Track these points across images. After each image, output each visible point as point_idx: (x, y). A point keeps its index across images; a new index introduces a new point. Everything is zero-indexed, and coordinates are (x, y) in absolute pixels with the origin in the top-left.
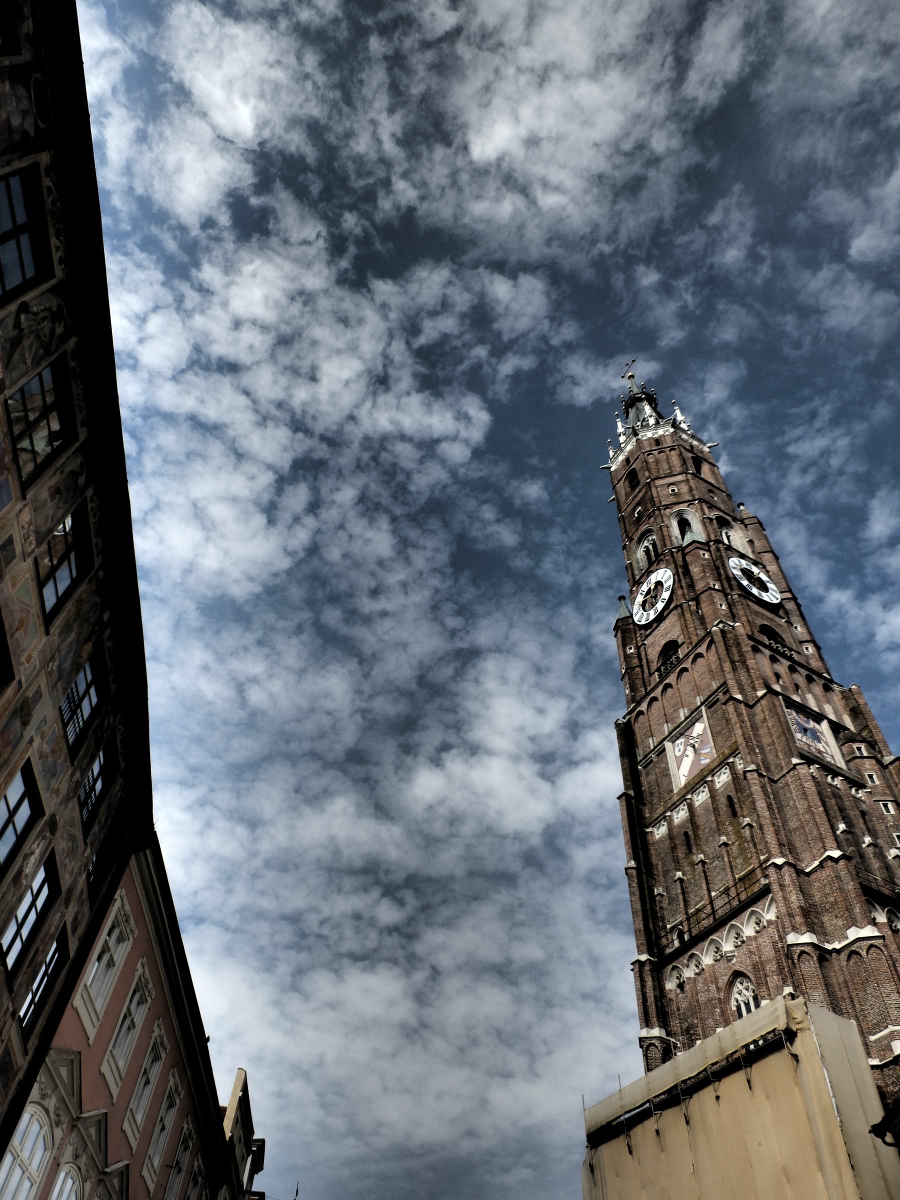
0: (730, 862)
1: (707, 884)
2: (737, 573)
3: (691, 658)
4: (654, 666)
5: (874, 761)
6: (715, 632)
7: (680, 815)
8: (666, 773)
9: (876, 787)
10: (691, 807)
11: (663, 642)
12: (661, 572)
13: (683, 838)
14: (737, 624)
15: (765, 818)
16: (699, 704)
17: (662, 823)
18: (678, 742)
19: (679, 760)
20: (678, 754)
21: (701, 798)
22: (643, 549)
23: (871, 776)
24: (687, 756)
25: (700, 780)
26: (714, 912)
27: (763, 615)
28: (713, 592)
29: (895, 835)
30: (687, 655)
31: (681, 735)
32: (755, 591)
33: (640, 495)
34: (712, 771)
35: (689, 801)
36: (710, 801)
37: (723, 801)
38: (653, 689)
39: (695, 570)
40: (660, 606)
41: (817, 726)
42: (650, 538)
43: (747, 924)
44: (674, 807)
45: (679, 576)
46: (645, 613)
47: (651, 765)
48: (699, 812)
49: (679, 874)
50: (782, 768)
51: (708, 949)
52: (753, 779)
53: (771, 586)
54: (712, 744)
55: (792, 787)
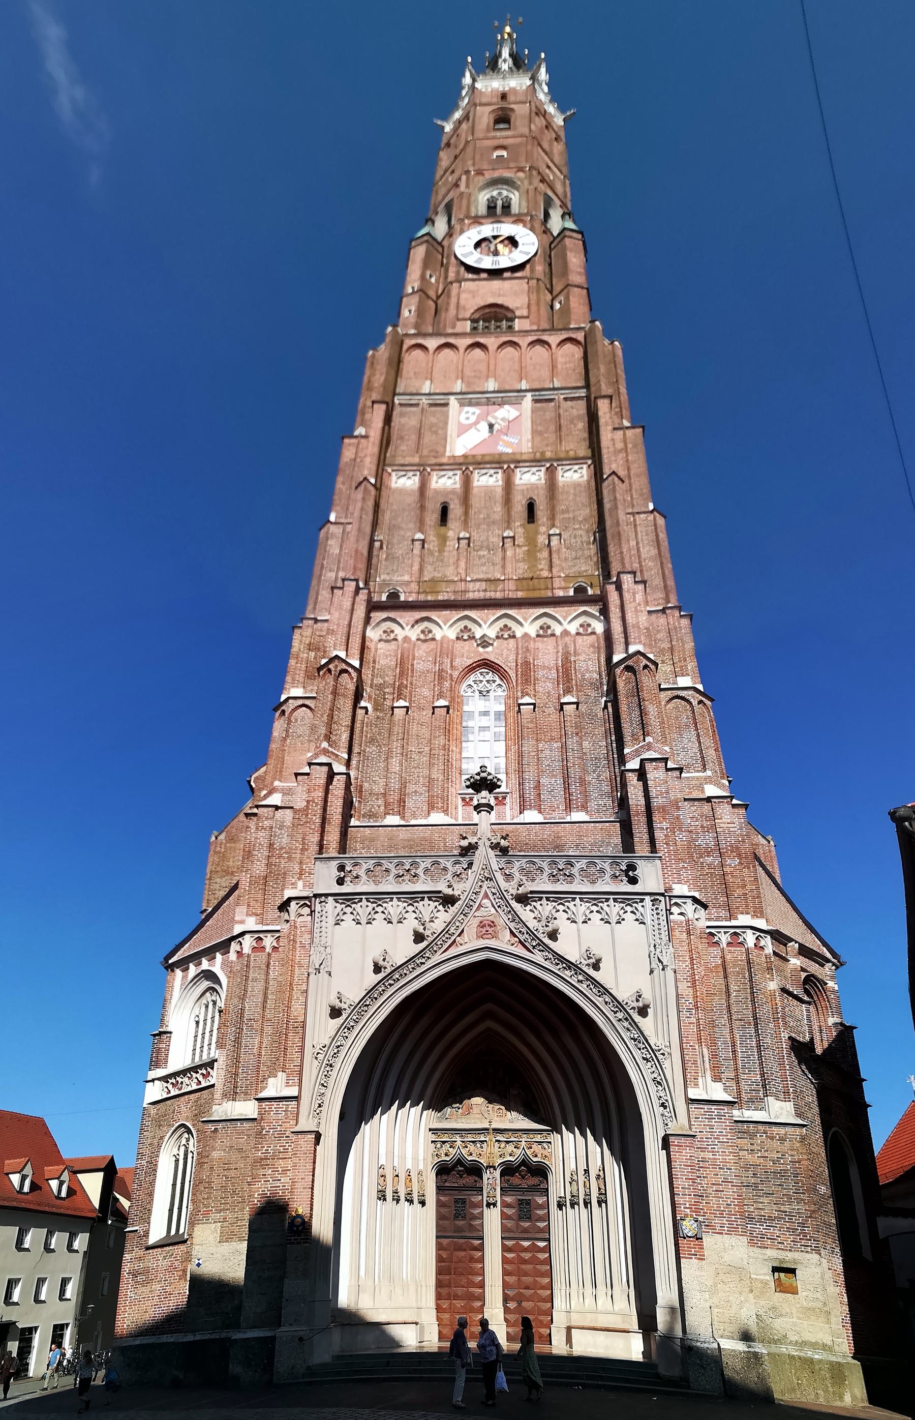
10: (467, 482)
13: (439, 507)
19: (463, 429)
20: (463, 420)
34: (519, 462)
48: (475, 491)
51: (455, 622)
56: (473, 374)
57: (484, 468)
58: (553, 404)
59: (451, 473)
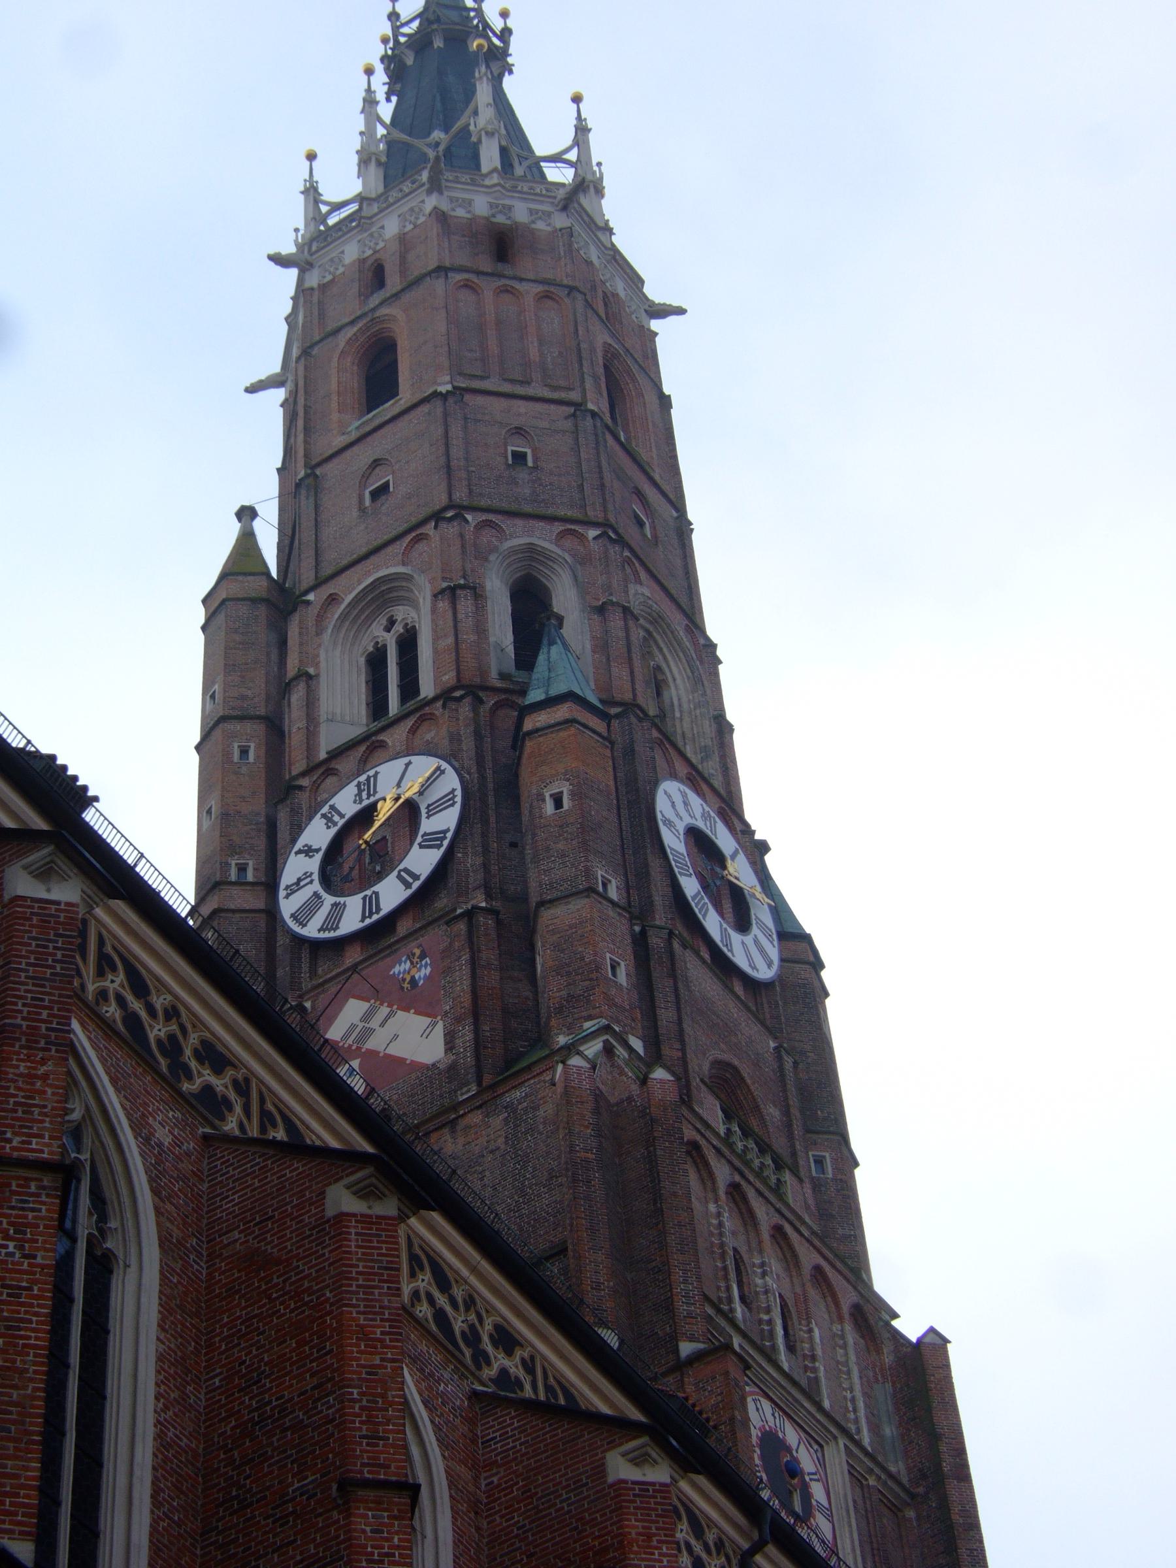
2: (674, 842)
32: (712, 923)
40: (391, 893)
46: (329, 900)
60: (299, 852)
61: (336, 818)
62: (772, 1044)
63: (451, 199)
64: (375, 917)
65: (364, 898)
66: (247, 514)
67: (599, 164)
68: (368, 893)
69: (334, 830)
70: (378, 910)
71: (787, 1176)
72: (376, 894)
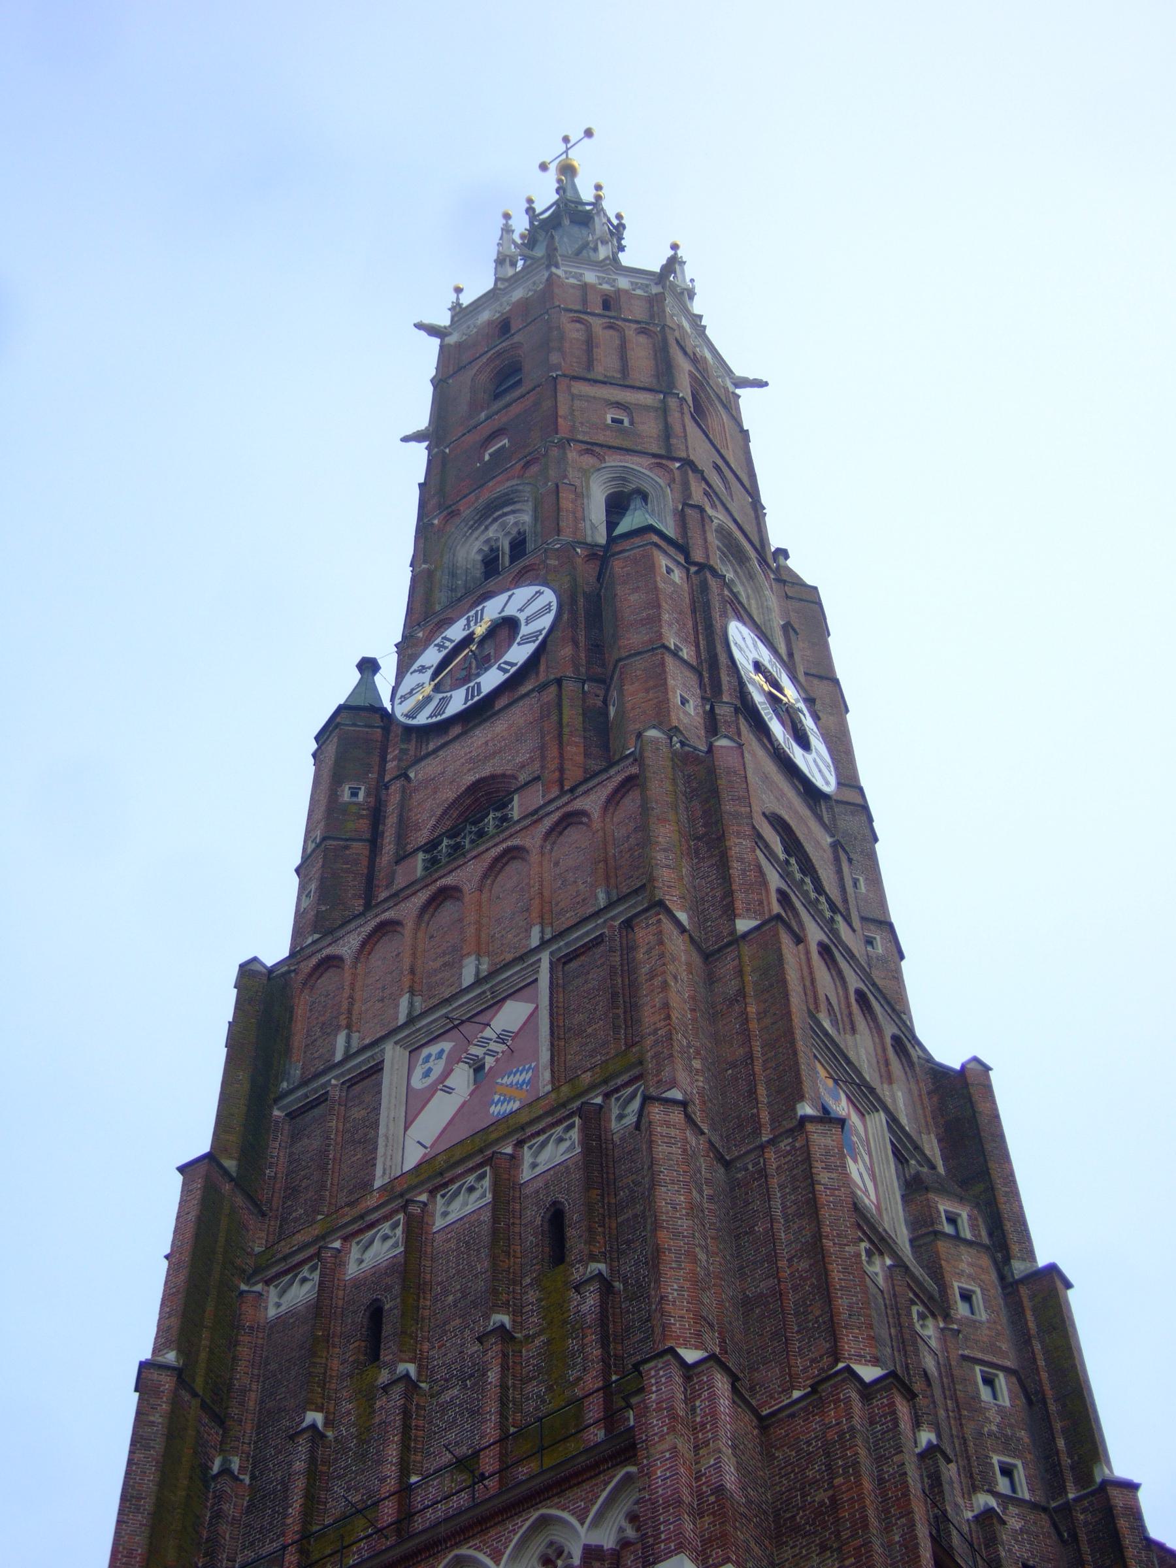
0: (503, 1387)
1: (406, 1448)
3: (548, 823)
4: (422, 837)
5: (985, 1261)
6: (655, 741)
7: (378, 1251)
8: (365, 1137)
9: (974, 1324)
10: (416, 1231)
11: (470, 779)
12: (523, 593)
13: (361, 1318)
14: (723, 742)
15: (676, 1235)
16: (535, 941)
17: (305, 1272)
18: (433, 1049)
19: (415, 1103)
20: (418, 1082)
21: (462, 1207)
22: (478, 545)
23: (966, 1297)
24: (449, 1090)
25: (478, 1151)
26: (406, 1515)
27: (783, 794)
28: (669, 660)
29: (995, 1459)
30: (535, 816)
31: (453, 1026)
33: (515, 409)
35: (415, 1209)
36: (486, 1216)
37: (533, 1216)
38: (397, 897)
39: (633, 598)
40: (491, 680)
41: (855, 1119)
42: (511, 519)
43: (514, 1557)
44: (364, 1226)
45: (573, 612)
47: (316, 1112)
49: (315, 1417)
50: (757, 1132)
52: (667, 1124)
53: (816, 742)
54: (545, 1055)
55: (774, 1182)
56: (440, 962)
57: (452, 1181)
58: (602, 948)
59: (385, 1228)
60: (415, 671)
61: (447, 644)
62: (829, 840)
63: (566, 272)
64: (476, 699)
65: (467, 690)
66: (368, 666)
67: (692, 280)
68: (471, 684)
69: (445, 652)
70: (479, 692)
71: (838, 918)
72: (479, 684)
